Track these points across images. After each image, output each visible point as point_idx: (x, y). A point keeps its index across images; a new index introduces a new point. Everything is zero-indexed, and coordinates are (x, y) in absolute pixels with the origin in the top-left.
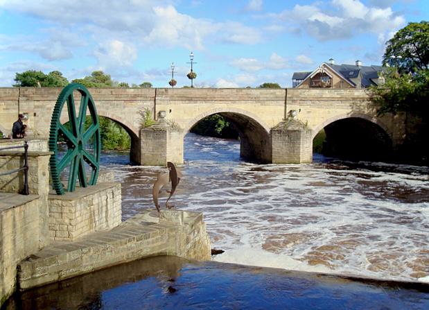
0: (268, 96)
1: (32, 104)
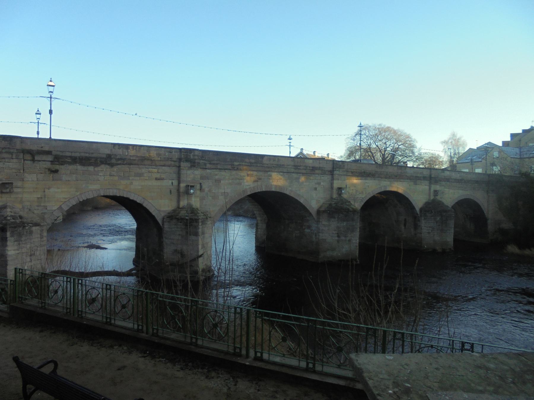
0: (418, 175)
1: (198, 172)
